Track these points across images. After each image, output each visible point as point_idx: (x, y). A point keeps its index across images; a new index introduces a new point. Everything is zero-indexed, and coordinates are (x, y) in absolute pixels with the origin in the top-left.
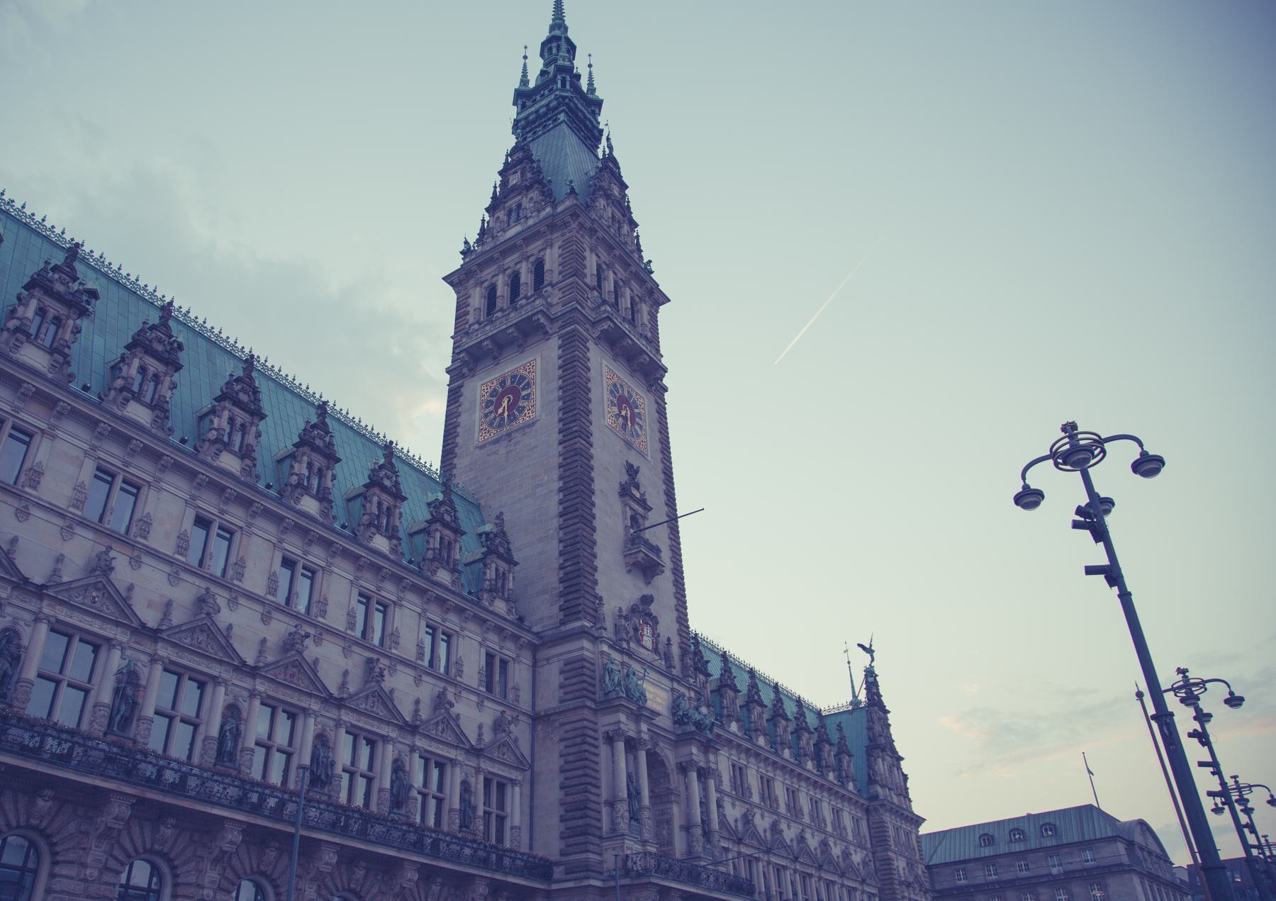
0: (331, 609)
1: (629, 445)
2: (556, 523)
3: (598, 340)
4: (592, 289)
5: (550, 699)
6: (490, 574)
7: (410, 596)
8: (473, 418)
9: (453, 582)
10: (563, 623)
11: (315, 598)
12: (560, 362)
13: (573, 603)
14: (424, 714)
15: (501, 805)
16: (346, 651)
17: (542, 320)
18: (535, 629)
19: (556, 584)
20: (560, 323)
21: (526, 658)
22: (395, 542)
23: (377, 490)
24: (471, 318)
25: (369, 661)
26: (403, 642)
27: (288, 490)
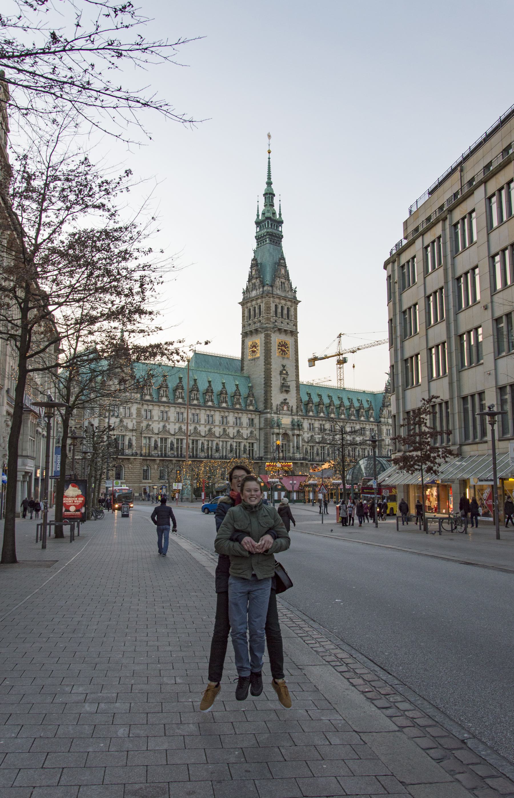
0: (216, 422)
1: (283, 358)
2: (263, 386)
5: (262, 425)
6: (249, 401)
7: (231, 413)
8: (248, 351)
10: (264, 410)
15: (253, 447)
16: (220, 428)
17: (260, 330)
18: (260, 410)
20: (264, 330)
21: (258, 417)
24: (245, 318)
25: (224, 429)
27: (205, 402)
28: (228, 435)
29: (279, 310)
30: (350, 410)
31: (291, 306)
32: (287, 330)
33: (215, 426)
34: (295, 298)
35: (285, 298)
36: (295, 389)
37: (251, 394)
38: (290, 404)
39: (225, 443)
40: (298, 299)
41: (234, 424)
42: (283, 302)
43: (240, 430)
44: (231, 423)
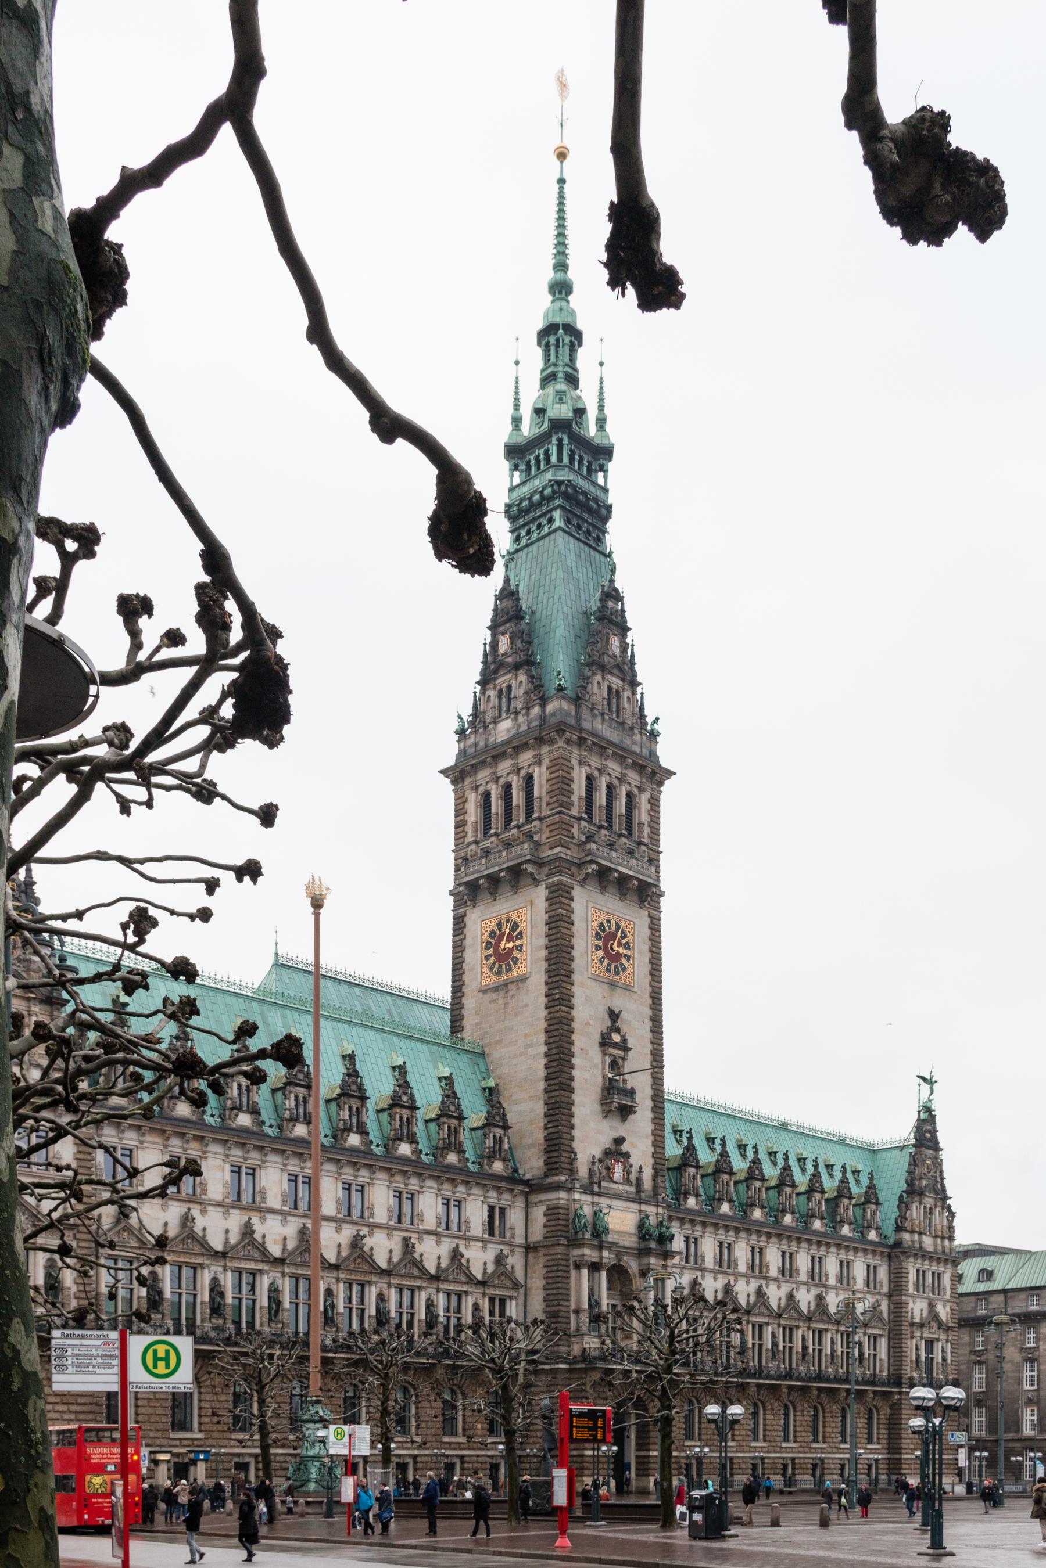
1: (612, 985)
2: (542, 1085)
3: (583, 883)
4: (580, 819)
9: (460, 1160)
10: (546, 1176)
11: (366, 1206)
12: (546, 917)
13: (553, 1160)
14: (443, 1265)
16: (389, 1236)
17: (530, 868)
19: (542, 1140)
20: (545, 870)
22: (414, 1146)
23: (398, 1110)
25: (406, 1240)
26: (426, 1218)
28: (418, 1264)
29: (600, 798)
30: (809, 1199)
31: (641, 789)
32: (630, 877)
33: (374, 1227)
34: (653, 754)
35: (622, 755)
36: (649, 1104)
37: (496, 1117)
38: (632, 1160)
39: (406, 1294)
40: (665, 762)
41: (439, 1225)
42: (614, 767)
43: (462, 1249)
44: (430, 1222)
